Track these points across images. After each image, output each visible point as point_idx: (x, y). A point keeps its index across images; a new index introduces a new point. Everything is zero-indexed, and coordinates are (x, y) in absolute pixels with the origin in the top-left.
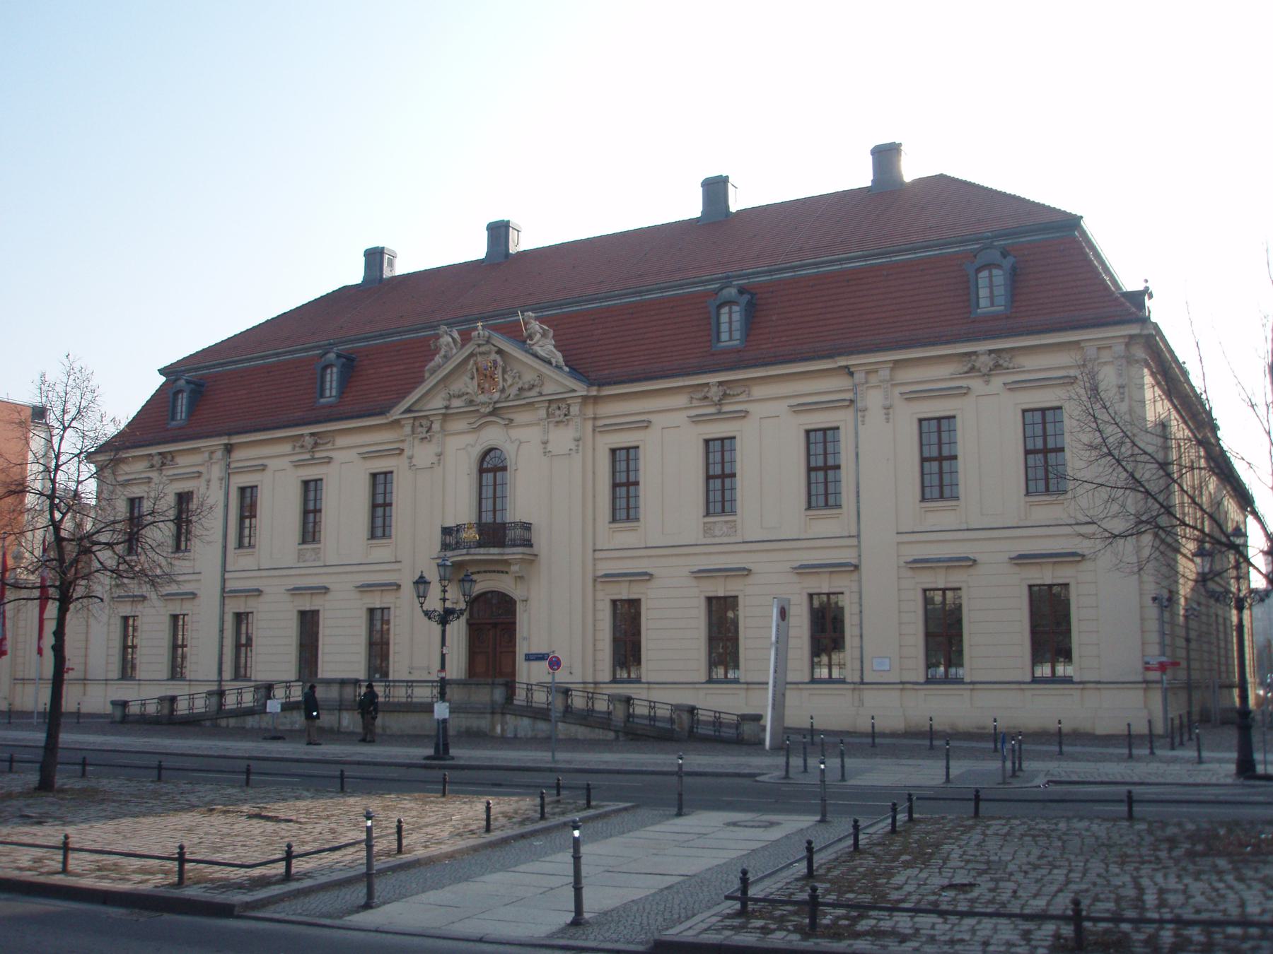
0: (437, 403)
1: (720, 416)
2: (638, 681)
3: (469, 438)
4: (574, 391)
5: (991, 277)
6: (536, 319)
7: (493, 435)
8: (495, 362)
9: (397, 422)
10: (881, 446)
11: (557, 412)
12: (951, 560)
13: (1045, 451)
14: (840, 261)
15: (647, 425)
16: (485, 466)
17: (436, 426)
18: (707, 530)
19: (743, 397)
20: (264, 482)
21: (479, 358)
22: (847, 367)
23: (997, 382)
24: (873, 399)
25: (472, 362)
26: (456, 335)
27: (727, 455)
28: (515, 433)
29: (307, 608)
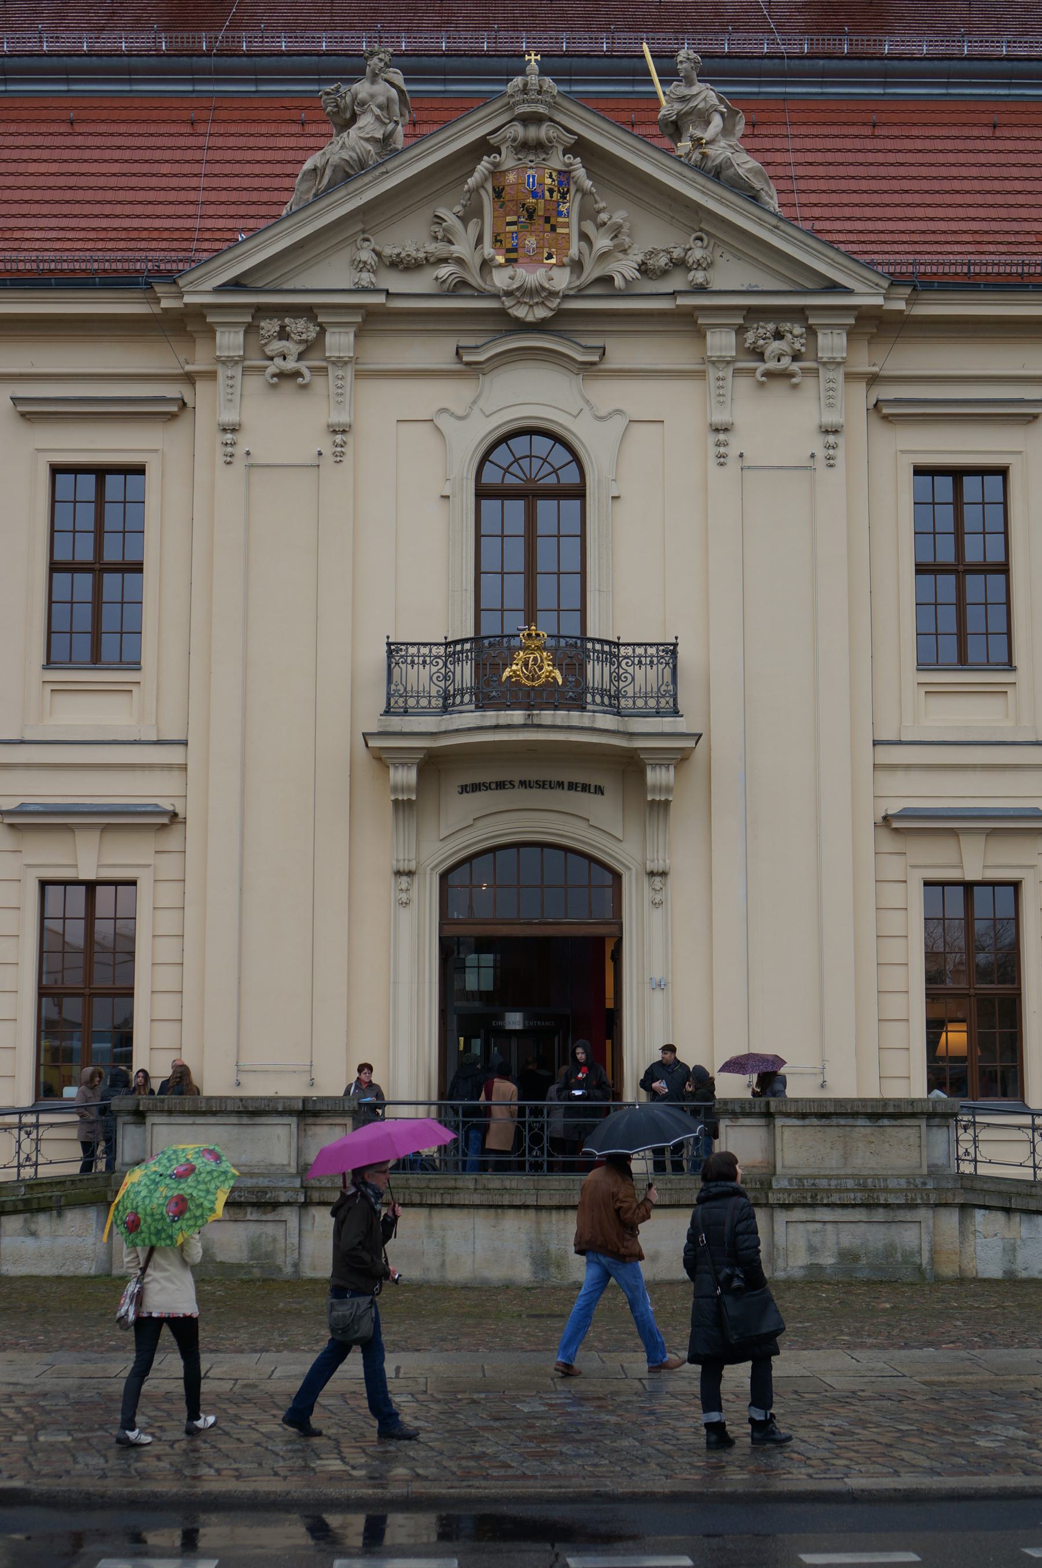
0: (333, 276)
3: (452, 394)
4: (833, 288)
6: (712, 69)
7: (531, 393)
8: (565, 175)
9: (199, 312)
11: (776, 346)
16: (492, 476)
17: (339, 342)
21: (507, 160)
25: (484, 166)
26: (399, 78)
28: (608, 394)
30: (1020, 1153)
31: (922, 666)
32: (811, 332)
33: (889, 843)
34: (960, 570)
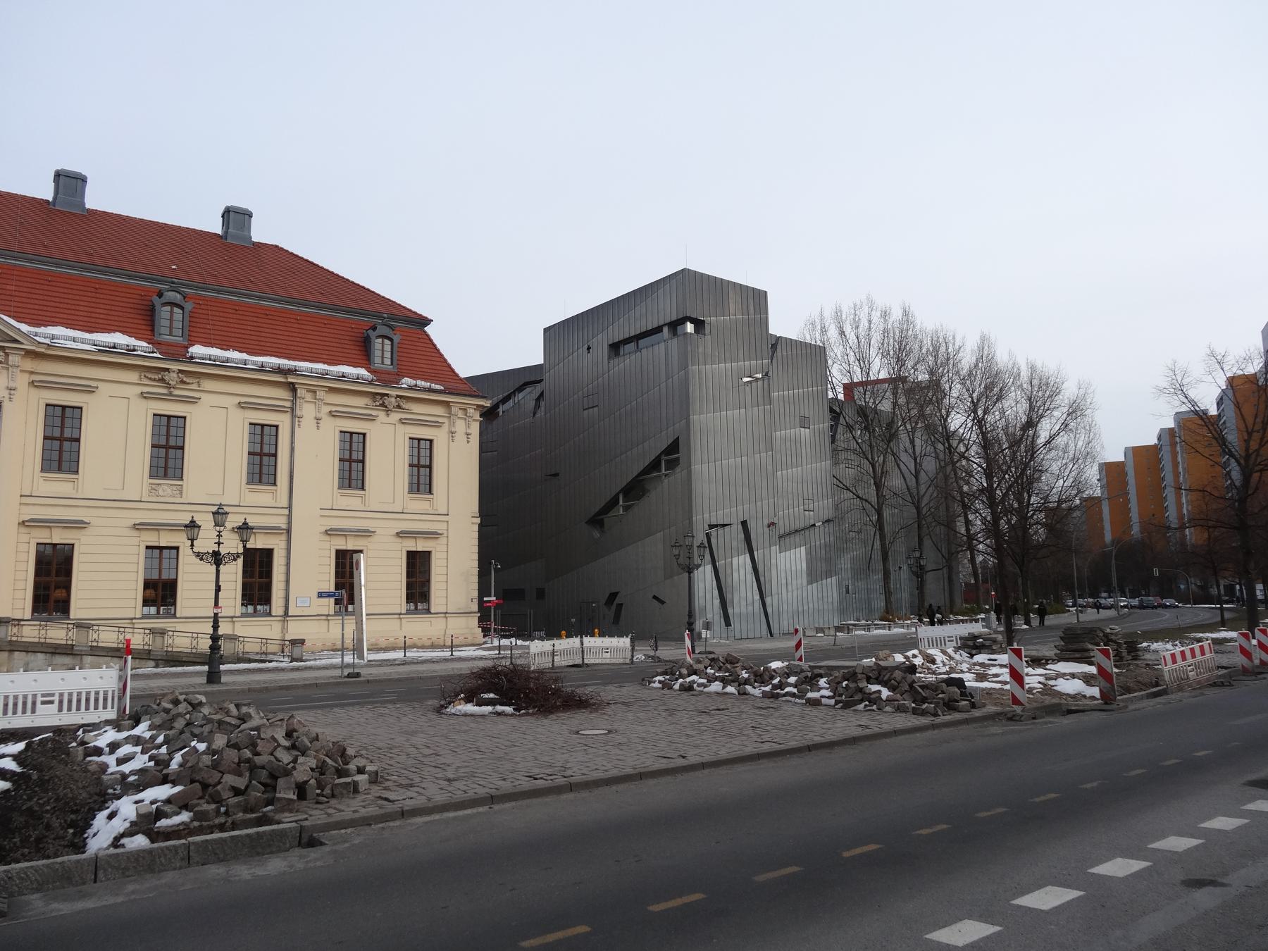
1: (170, 398)
2: (174, 616)
5: (172, 312)
10: (313, 445)
12: (359, 531)
13: (61, 439)
14: (260, 298)
15: (90, 391)
18: (153, 489)
19: (194, 387)
20: (440, 437)
22: (292, 383)
23: (395, 416)
24: (307, 410)
27: (416, 453)
29: (344, 548)
30: (36, 633)
31: (42, 470)
32: (7, 355)
33: (23, 530)
34: (61, 439)
